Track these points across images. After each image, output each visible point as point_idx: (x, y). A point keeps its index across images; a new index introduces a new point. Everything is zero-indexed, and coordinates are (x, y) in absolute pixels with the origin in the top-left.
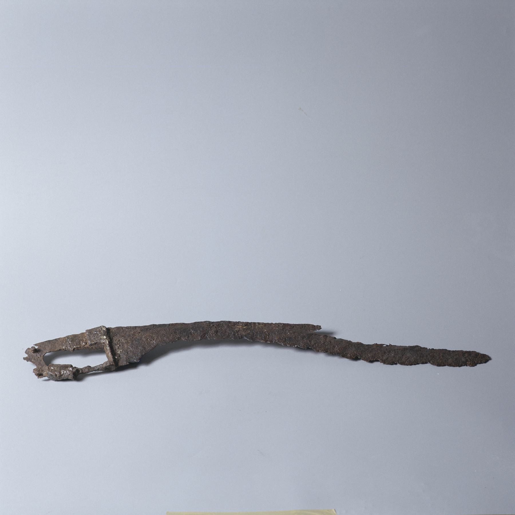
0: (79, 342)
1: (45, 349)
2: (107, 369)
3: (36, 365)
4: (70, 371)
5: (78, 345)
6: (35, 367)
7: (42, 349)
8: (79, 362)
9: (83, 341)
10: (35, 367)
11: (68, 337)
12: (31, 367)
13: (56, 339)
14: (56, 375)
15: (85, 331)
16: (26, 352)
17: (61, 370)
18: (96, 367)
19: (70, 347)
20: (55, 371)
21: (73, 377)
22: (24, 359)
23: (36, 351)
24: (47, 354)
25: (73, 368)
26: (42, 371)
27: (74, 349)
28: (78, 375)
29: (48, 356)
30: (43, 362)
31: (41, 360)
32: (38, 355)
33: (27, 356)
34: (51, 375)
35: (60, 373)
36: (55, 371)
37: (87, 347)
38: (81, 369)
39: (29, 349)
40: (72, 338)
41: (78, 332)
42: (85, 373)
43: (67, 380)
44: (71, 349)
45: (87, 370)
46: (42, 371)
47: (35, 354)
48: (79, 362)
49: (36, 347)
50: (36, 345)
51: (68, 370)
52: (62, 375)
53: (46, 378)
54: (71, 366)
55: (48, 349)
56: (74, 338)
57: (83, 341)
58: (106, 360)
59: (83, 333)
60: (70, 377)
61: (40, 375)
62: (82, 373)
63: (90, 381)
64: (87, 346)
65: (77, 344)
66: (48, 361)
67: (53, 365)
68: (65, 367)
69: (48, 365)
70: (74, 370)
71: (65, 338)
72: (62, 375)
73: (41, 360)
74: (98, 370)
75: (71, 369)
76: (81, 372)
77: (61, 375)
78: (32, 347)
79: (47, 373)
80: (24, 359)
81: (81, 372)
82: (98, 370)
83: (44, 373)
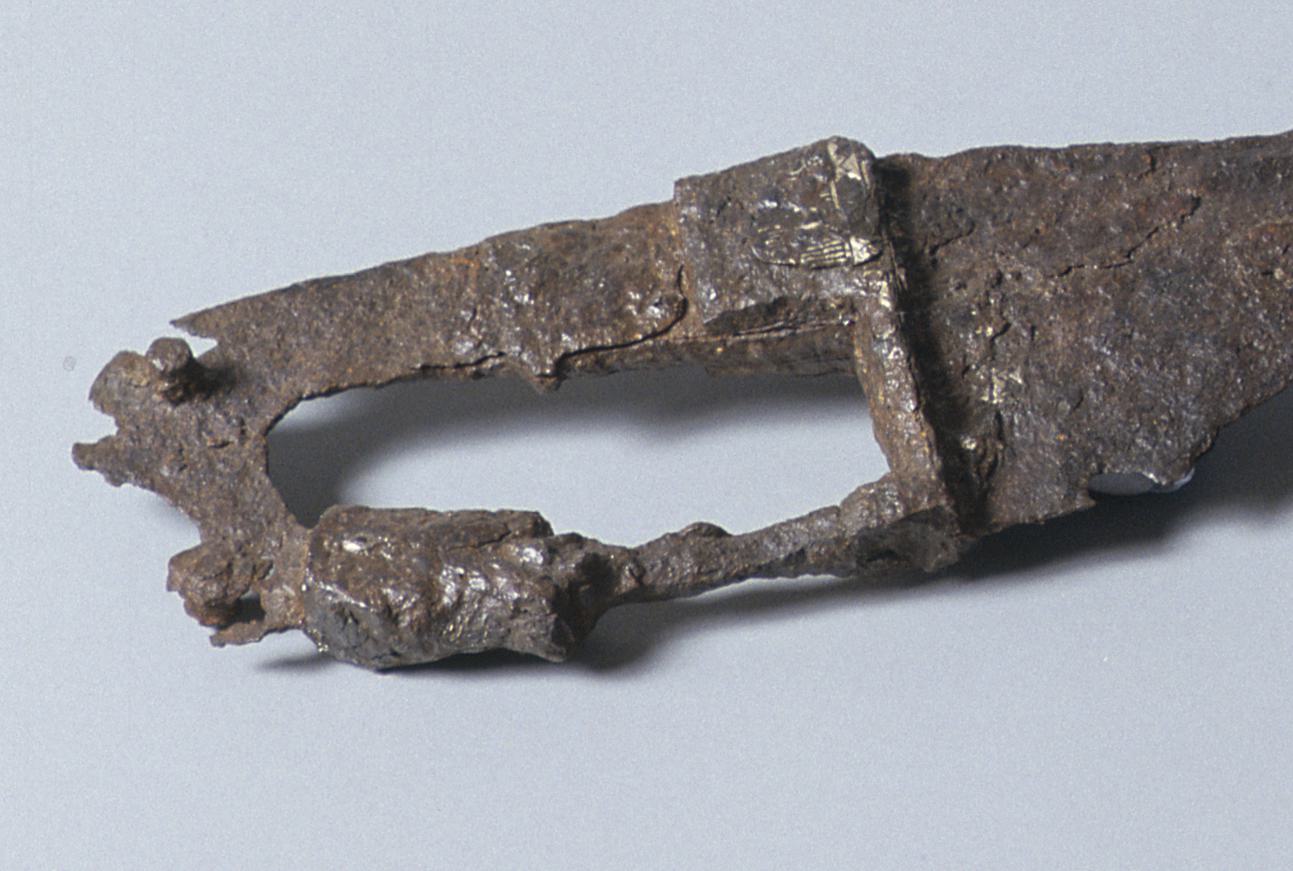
0: (616, 294)
1: (285, 363)
2: (877, 559)
3: (201, 519)
4: (525, 571)
5: (615, 318)
6: (189, 538)
7: (254, 362)
8: (609, 486)
9: (646, 281)
10: (189, 538)
11: (503, 247)
12: (149, 531)
13: (387, 271)
14: (389, 614)
15: (665, 194)
16: (101, 395)
17: (433, 562)
18: (772, 533)
19: (527, 339)
20: (381, 572)
21: (558, 636)
22: (85, 455)
23: (194, 381)
24: (304, 413)
25: (554, 548)
26: (260, 571)
27: (562, 366)
28: (601, 614)
29: (312, 436)
30: (259, 487)
31: (243, 473)
32: (219, 419)
33: (102, 427)
34: (342, 612)
35: (429, 591)
36: (381, 572)
37: (691, 345)
38: (634, 555)
39: (126, 360)
40: (541, 259)
41: (597, 199)
42: (671, 593)
43: (494, 659)
44: (535, 365)
45: (688, 566)
46: (260, 571)
47: (184, 415)
48: (609, 486)
49: (201, 347)
50: (195, 323)
51: (510, 567)
52: (447, 615)
53: (296, 642)
54: (538, 528)
55: (310, 363)
56: (561, 258)
57: (646, 281)
58: (113, 431)
59: (649, 211)
60: (525, 635)
61: (233, 613)
62: (643, 593)
63: (720, 671)
64: (691, 329)
65: (587, 311)
66: (313, 478)
67: (361, 520)
68: (481, 535)
69: (308, 519)
70: (568, 566)
71: (473, 252)
72: (447, 615)
73: (243, 473)
74: (797, 561)
75: (532, 555)
76: (627, 583)
77: (436, 618)
78: (160, 347)
79: (306, 599)
80: (85, 455)
81: (627, 583)
82: (797, 561)
83: (278, 598)
